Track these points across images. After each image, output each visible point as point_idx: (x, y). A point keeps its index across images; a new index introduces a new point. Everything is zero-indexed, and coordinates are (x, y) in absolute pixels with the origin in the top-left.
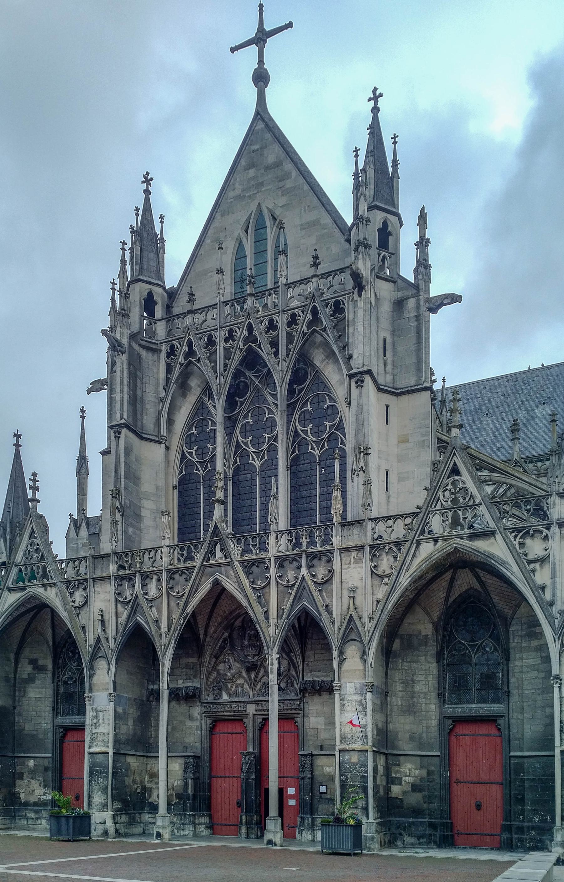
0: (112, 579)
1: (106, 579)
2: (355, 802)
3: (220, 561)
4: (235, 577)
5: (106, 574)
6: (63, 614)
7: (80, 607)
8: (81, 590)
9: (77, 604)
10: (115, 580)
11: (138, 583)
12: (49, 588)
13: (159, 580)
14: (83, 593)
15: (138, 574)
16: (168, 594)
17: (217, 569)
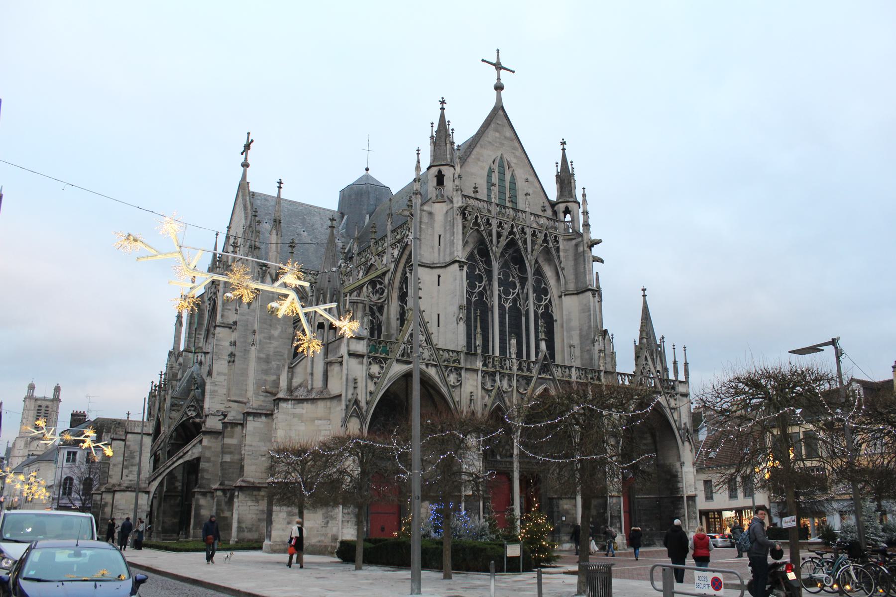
0: (480, 373)
1: (476, 371)
2: (616, 525)
3: (547, 377)
4: (555, 389)
5: (473, 367)
6: (444, 390)
7: (454, 387)
8: (454, 373)
9: (452, 384)
10: (482, 372)
11: (498, 378)
12: (430, 367)
13: (510, 380)
14: (456, 376)
15: (498, 374)
16: (517, 390)
17: (544, 381)
